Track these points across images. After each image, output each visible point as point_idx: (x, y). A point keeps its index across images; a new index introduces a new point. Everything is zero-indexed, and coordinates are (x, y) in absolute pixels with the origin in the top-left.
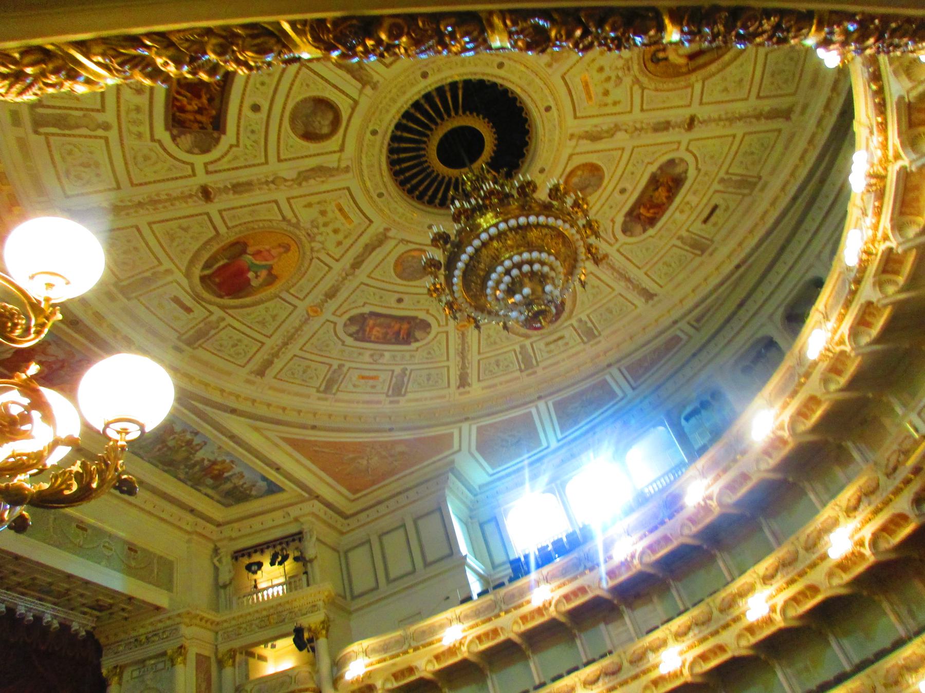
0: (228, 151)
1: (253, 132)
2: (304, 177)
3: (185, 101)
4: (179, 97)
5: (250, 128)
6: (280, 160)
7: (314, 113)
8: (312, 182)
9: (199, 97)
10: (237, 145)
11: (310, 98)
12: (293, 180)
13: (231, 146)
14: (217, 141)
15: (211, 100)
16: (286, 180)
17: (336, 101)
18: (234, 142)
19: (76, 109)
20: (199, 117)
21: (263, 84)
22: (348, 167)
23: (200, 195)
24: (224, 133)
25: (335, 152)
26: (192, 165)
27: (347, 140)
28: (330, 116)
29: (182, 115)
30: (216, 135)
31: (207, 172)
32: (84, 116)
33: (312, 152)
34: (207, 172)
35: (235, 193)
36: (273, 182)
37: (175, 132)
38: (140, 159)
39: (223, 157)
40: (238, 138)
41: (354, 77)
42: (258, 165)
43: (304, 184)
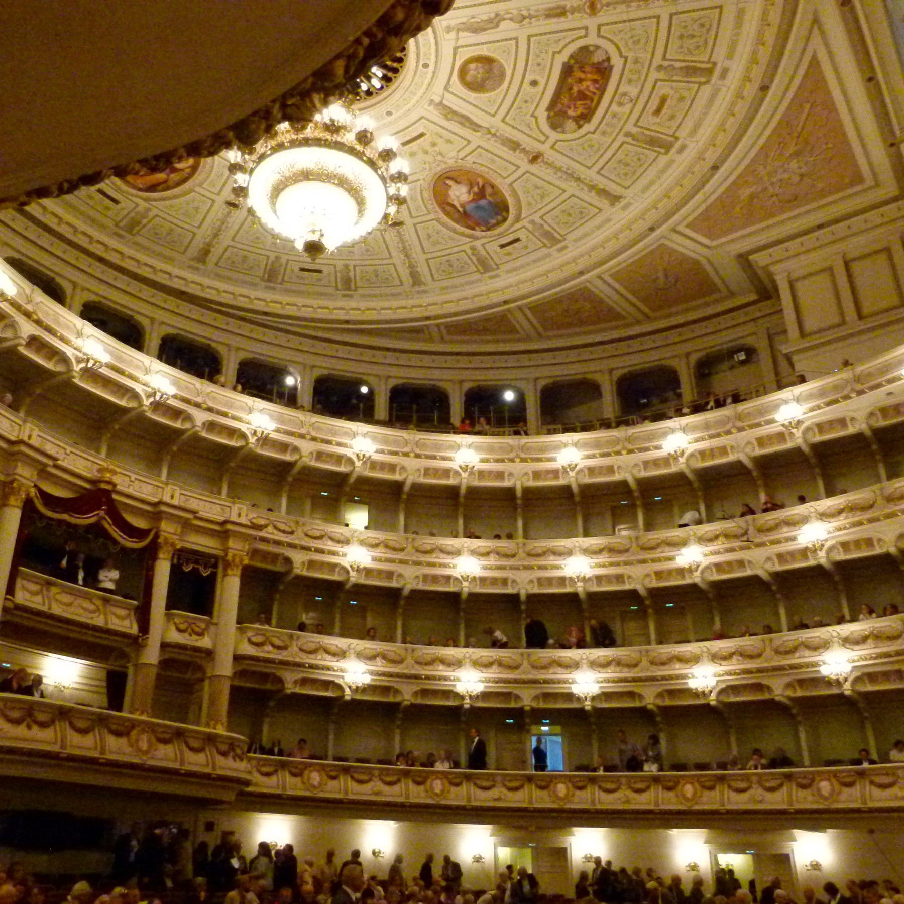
0: (563, 48)
1: (539, 65)
2: (494, 22)
3: (592, 88)
4: (595, 91)
5: (541, 67)
6: (516, 39)
7: (484, 80)
8: (485, 17)
9: (579, 92)
10: (554, 53)
11: (488, 91)
12: (504, 19)
13: (560, 52)
14: (571, 57)
15: (571, 89)
16: (511, 19)
17: (464, 90)
18: (557, 56)
19: (676, 81)
20: (582, 76)
21: (526, 102)
22: (448, 32)
23: (599, 6)
24: (564, 64)
25: (462, 47)
26: (599, 35)
27: (451, 60)
28: (469, 78)
29: (595, 77)
30: (572, 62)
31: (586, 28)
32: (672, 76)
33: (485, 46)
34: (586, 28)
35: (564, 7)
36: (524, 18)
37: (606, 64)
38: (643, 41)
39: (569, 43)
40: (553, 59)
41: (450, 108)
42: (537, 35)
43: (493, 15)
